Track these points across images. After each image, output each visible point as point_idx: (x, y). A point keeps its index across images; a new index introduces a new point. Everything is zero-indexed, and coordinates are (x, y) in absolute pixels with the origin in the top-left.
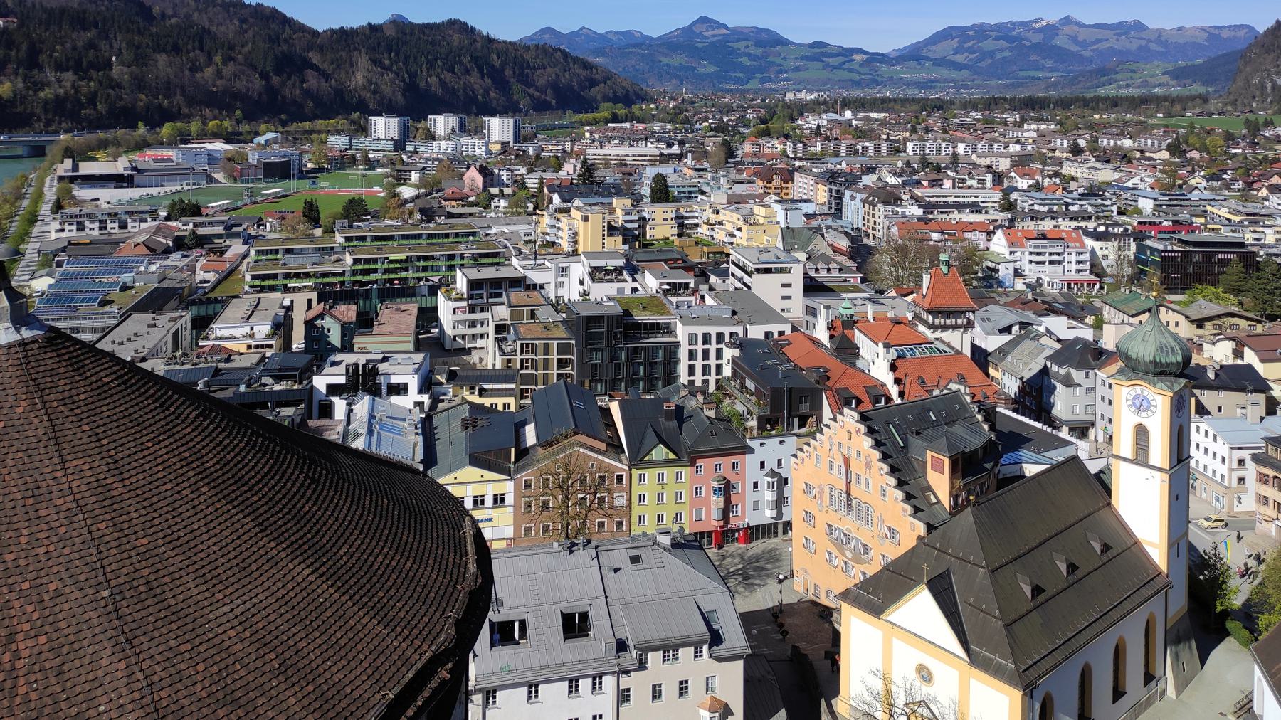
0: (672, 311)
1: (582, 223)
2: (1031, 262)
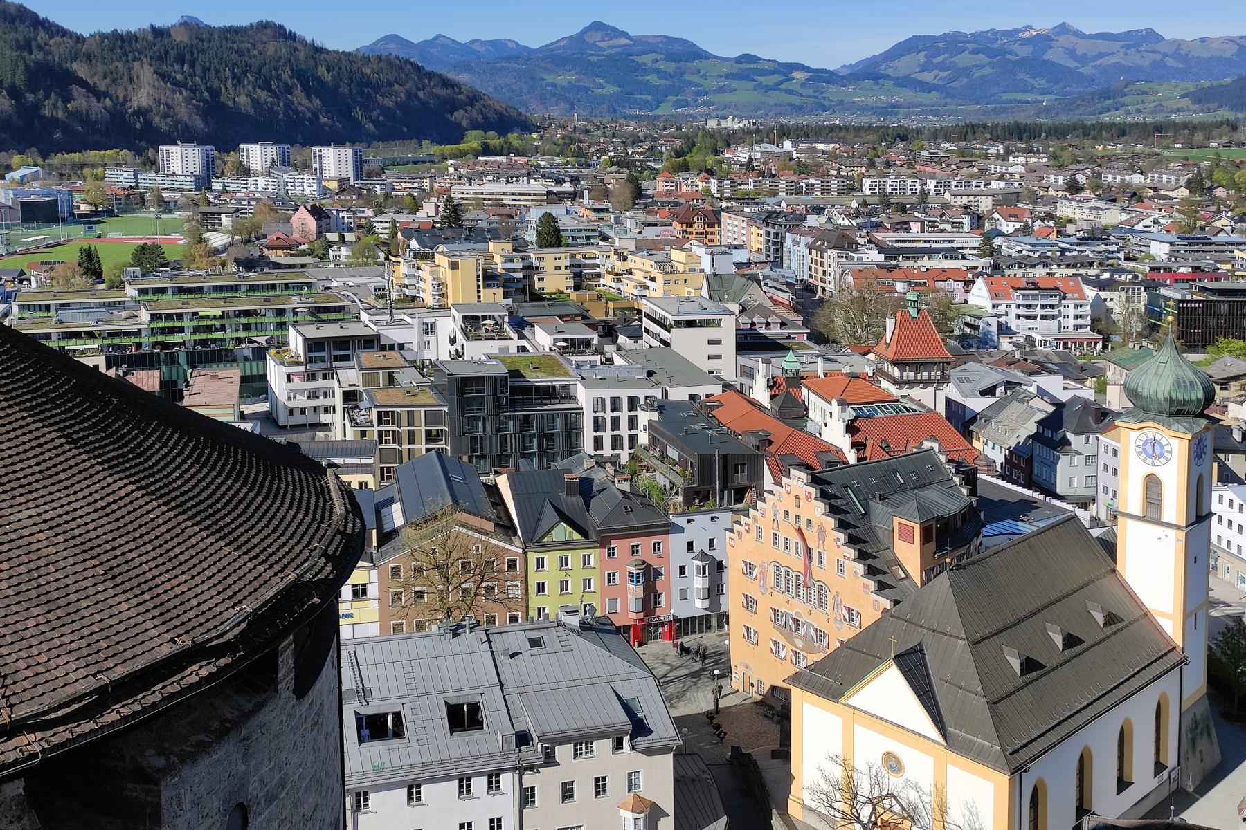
0: (571, 372)
1: (449, 271)
2: (1018, 316)
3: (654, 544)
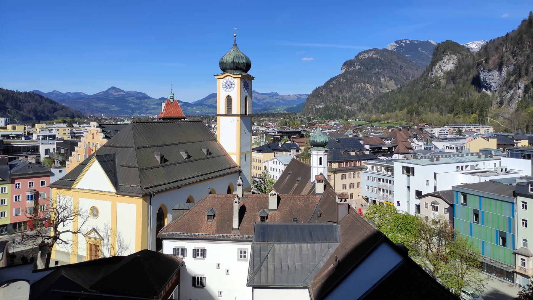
3: (42, 182)
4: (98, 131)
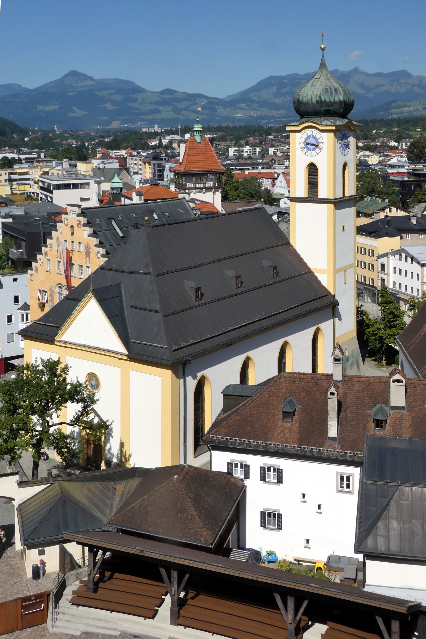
4: (80, 222)
